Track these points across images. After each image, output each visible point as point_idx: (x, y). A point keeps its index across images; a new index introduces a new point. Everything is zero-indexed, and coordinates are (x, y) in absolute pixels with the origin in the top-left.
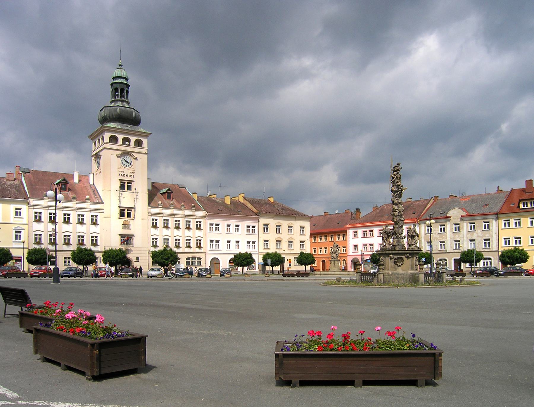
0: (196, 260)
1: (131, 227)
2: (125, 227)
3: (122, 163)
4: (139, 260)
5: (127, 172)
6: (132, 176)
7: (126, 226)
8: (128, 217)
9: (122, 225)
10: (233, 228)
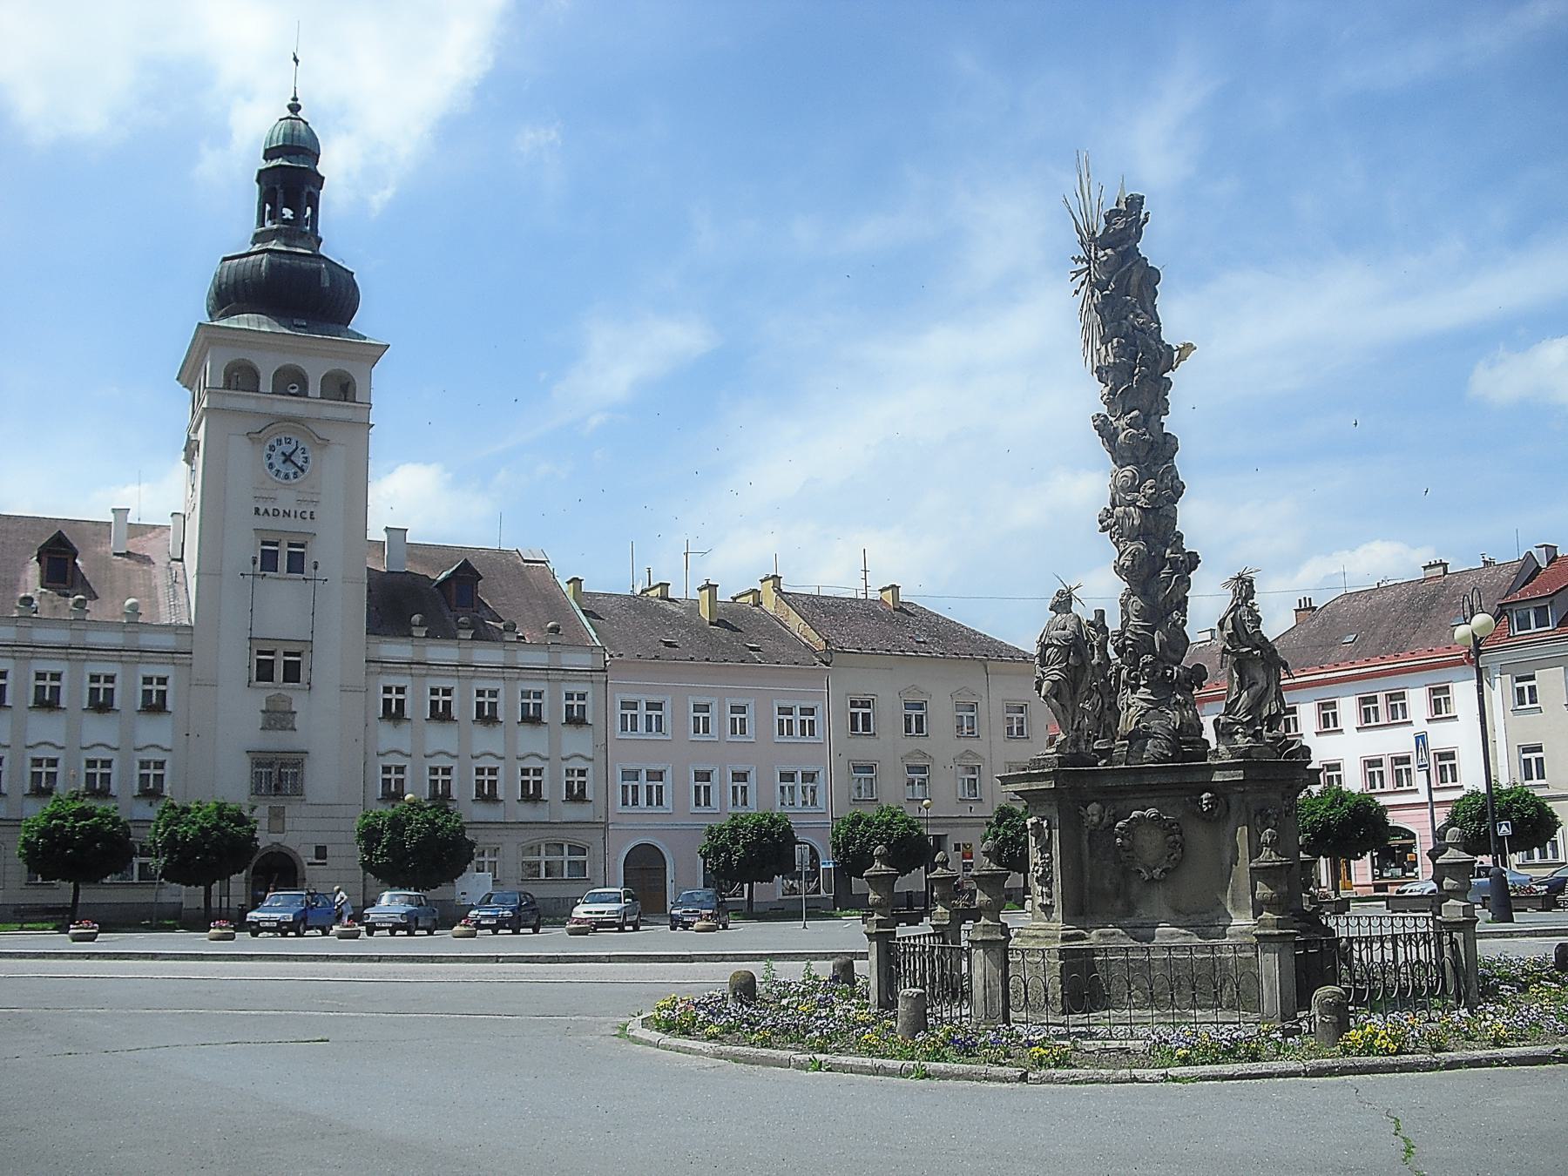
1: (298, 721)
5: (286, 499)
7: (279, 717)
9: (263, 711)
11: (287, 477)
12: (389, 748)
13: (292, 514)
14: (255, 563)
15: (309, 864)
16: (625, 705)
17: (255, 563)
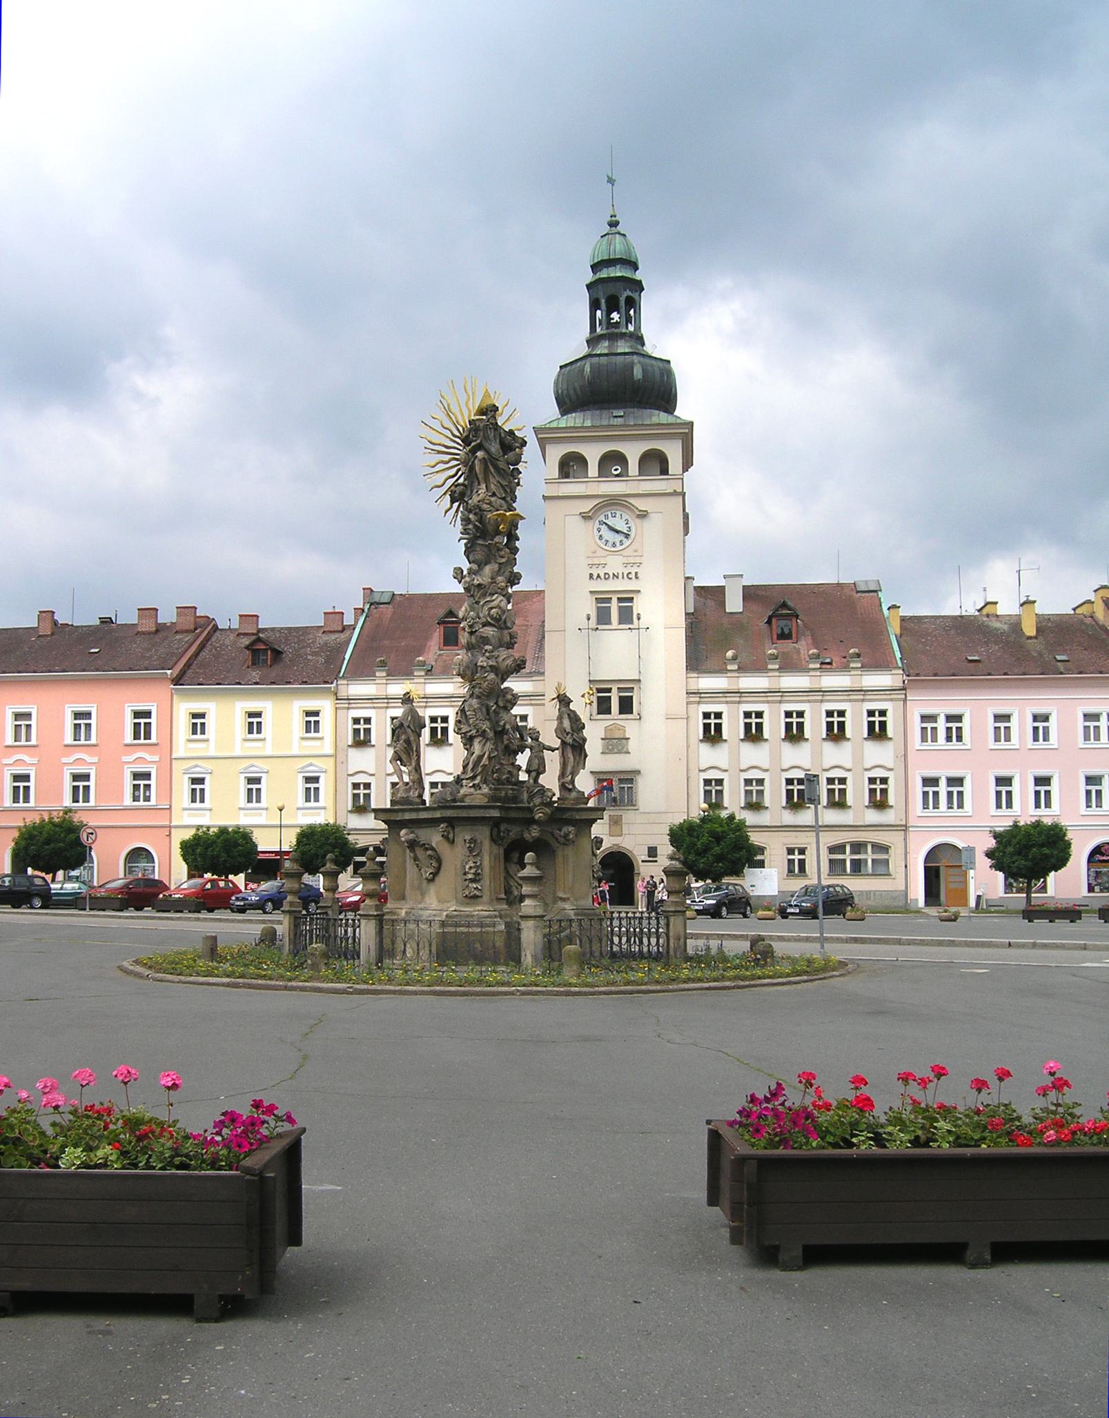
0: (869, 856)
1: (632, 745)
2: (610, 747)
3: (601, 536)
4: (656, 857)
5: (615, 564)
6: (633, 576)
8: (620, 713)
9: (602, 739)
10: (1020, 726)
11: (614, 545)
12: (833, 764)
13: (620, 576)
14: (589, 619)
15: (643, 861)
16: (924, 718)
17: (589, 619)
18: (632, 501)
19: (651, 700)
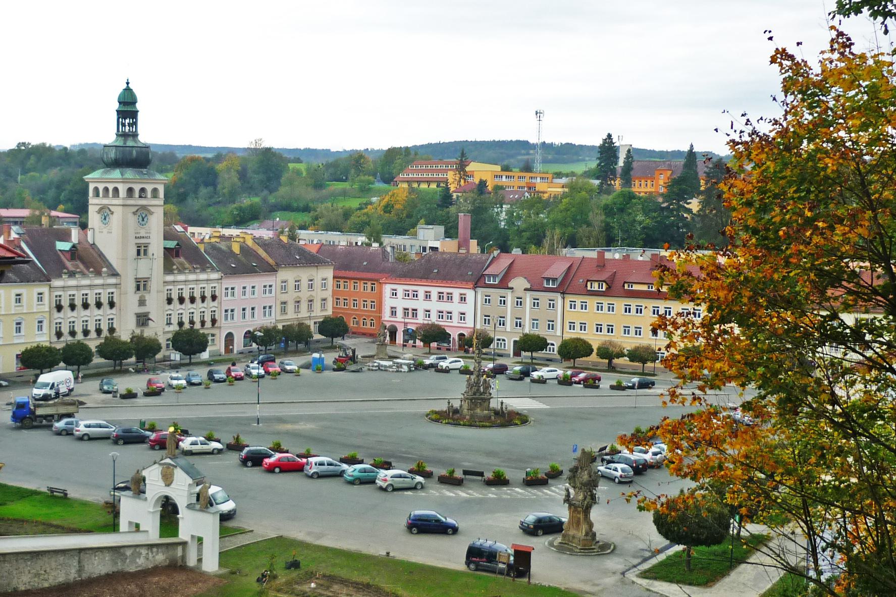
1: (147, 303)
5: (143, 234)
7: (142, 302)
18: (149, 208)
19: (154, 285)
